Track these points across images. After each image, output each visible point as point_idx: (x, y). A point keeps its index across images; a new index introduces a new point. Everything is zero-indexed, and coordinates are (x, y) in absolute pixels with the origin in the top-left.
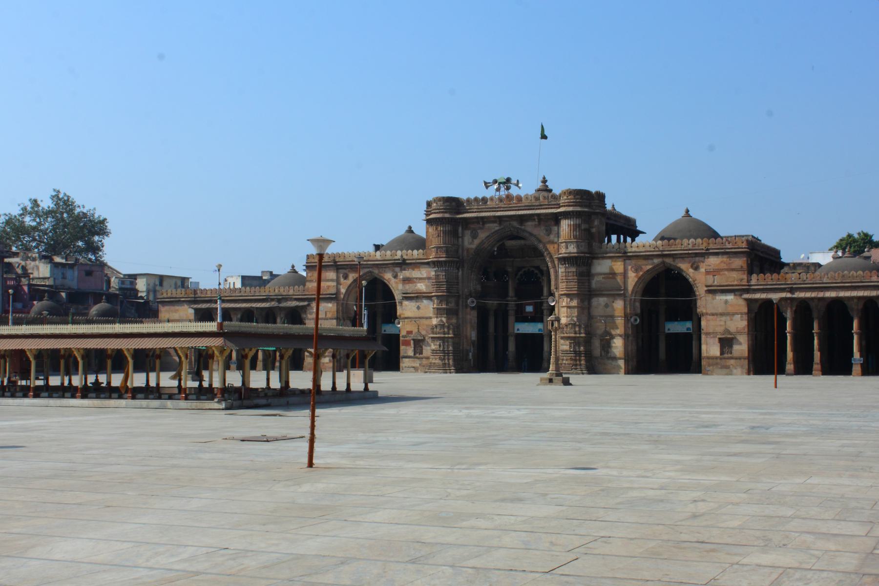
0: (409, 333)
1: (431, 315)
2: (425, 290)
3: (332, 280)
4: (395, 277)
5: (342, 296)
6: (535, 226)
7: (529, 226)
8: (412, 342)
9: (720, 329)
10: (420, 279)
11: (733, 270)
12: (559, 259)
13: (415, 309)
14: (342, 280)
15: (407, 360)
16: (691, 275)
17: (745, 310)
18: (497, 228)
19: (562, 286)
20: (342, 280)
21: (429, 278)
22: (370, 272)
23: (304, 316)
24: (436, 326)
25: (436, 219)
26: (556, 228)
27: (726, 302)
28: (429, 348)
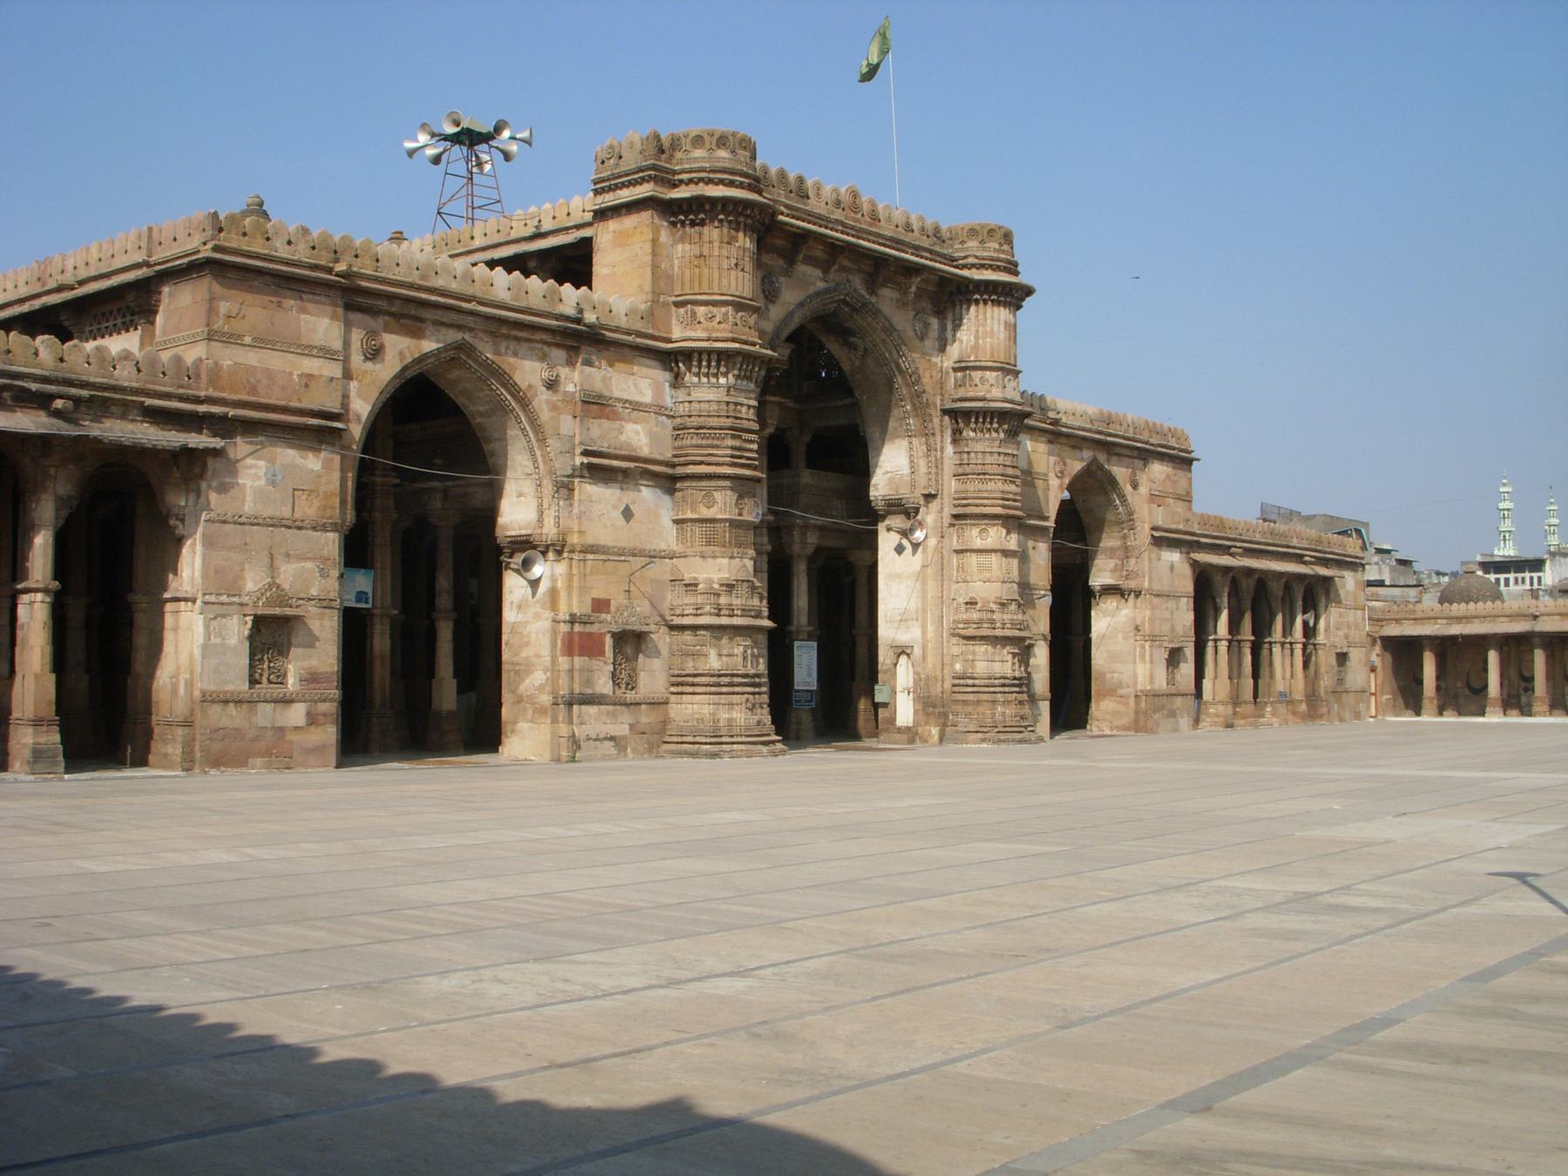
0: (601, 605)
1: (663, 546)
2: (645, 451)
3: (326, 353)
4: (552, 385)
5: (357, 431)
6: (902, 304)
7: (886, 298)
8: (609, 641)
9: (1166, 628)
10: (637, 407)
11: (1178, 498)
12: (945, 412)
13: (617, 514)
14: (357, 359)
15: (592, 710)
16: (1129, 498)
17: (1188, 587)
18: (821, 285)
19: (951, 486)
20: (357, 359)
21: (660, 410)
22: (460, 347)
23: (179, 501)
24: (730, 587)
25: (736, 202)
26: (934, 323)
27: (1172, 568)
28: (657, 664)
